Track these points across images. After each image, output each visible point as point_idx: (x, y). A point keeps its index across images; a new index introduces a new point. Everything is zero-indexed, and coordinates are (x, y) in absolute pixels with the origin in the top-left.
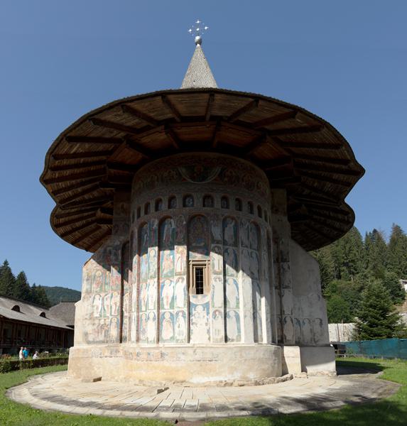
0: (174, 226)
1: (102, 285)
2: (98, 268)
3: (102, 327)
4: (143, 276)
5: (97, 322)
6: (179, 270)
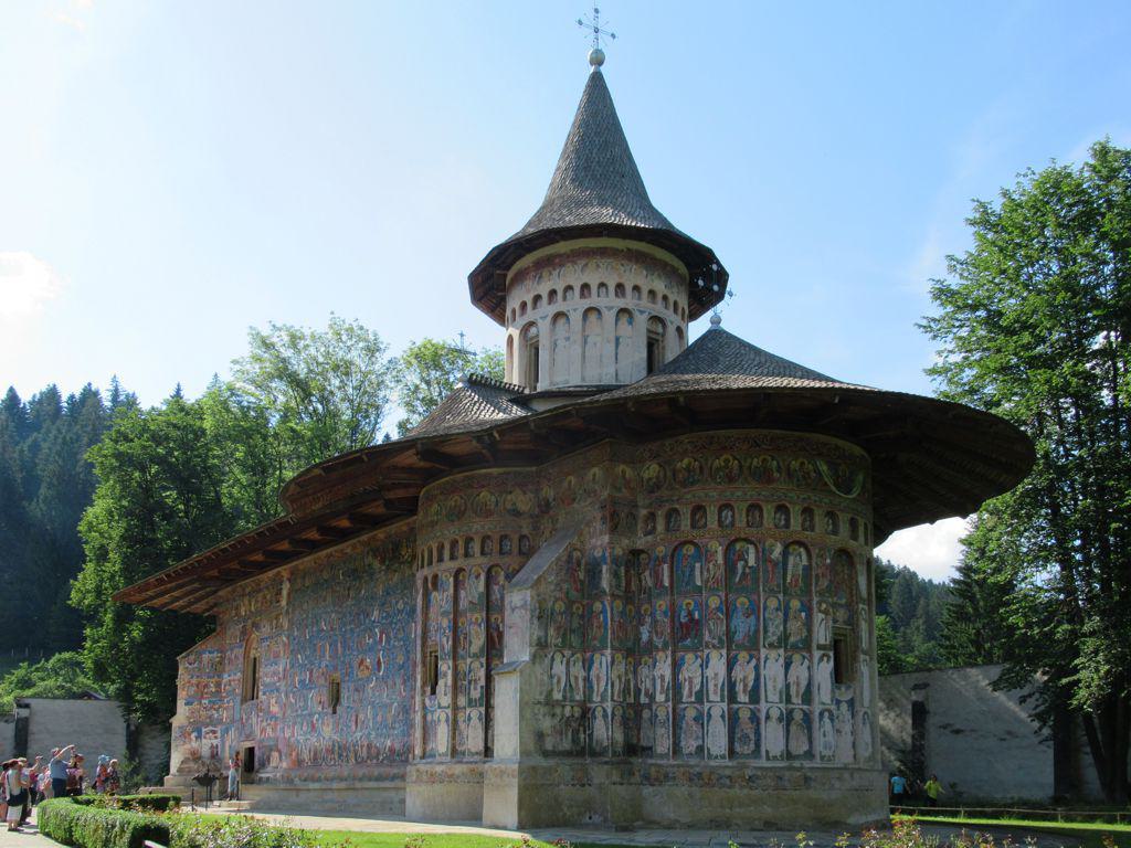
0: (805, 562)
1: (565, 633)
2: (558, 595)
3: (568, 722)
4: (739, 637)
5: (558, 711)
6: (822, 642)
